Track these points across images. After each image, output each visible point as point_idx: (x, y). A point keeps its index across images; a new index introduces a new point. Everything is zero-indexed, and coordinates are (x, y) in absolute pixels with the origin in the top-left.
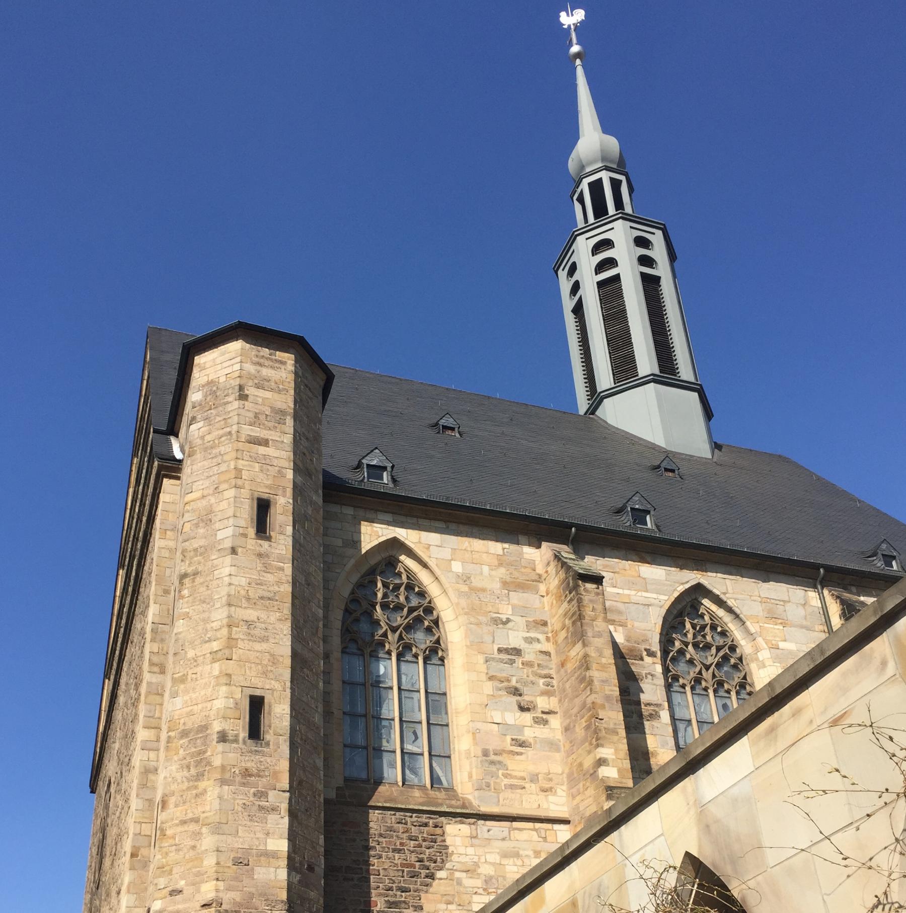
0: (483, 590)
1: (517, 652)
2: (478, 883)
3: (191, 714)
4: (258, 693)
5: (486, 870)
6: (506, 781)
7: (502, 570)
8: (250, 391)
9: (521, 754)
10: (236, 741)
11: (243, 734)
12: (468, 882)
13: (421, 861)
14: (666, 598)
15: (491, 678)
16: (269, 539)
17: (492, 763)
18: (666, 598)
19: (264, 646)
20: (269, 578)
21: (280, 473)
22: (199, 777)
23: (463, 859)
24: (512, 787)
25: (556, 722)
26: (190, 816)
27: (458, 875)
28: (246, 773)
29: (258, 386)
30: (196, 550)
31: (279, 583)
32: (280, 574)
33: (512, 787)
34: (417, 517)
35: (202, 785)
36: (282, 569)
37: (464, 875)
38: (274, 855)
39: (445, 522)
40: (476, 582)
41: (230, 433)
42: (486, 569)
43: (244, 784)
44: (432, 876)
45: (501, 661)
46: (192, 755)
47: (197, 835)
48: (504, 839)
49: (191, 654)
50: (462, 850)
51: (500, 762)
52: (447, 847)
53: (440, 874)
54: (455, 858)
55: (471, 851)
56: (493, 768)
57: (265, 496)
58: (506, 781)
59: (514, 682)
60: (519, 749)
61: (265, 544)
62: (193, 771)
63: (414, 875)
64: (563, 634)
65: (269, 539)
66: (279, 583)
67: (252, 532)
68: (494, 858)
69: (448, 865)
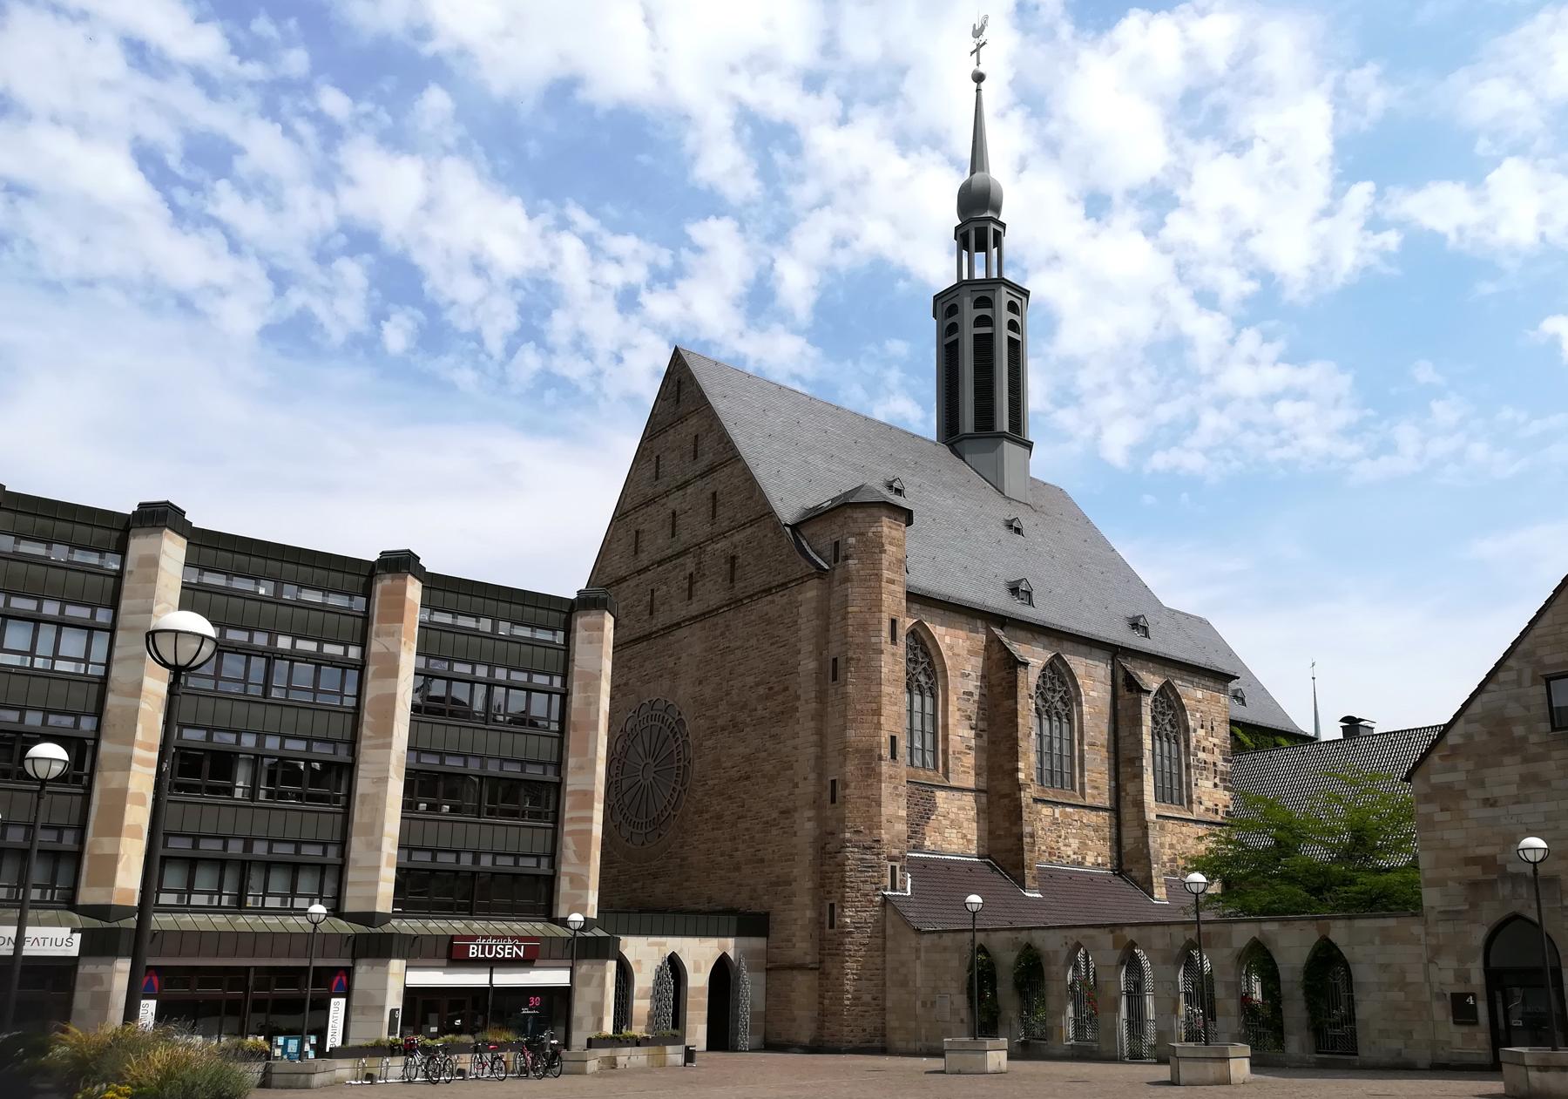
0: (959, 655)
1: (971, 694)
2: (948, 822)
3: (861, 741)
4: (893, 735)
5: (952, 816)
6: (962, 769)
7: (968, 642)
8: (887, 547)
9: (969, 754)
10: (886, 760)
11: (889, 757)
12: (944, 822)
13: (925, 810)
14: (1041, 662)
15: (959, 710)
16: (896, 644)
17: (956, 758)
18: (1041, 662)
19: (895, 708)
20: (897, 668)
21: (900, 602)
22: (868, 776)
23: (943, 810)
24: (964, 772)
25: (985, 736)
26: (864, 794)
27: (940, 818)
28: (891, 777)
29: (890, 544)
30: (857, 644)
31: (900, 671)
32: (901, 666)
33: (964, 772)
34: (931, 607)
35: (870, 781)
36: (901, 663)
37: (942, 818)
38: (901, 818)
39: (944, 610)
40: (956, 651)
41: (877, 574)
42: (961, 641)
43: (890, 783)
44: (929, 818)
45: (964, 699)
46: (864, 764)
47: (869, 806)
48: (959, 800)
49: (858, 707)
50: (942, 805)
51: (959, 758)
52: (936, 803)
53: (933, 817)
54: (939, 809)
55: (945, 806)
56: (957, 761)
57: (894, 617)
58: (962, 769)
59: (968, 713)
60: (969, 751)
61: (895, 647)
62: (865, 772)
63: (922, 817)
64: (999, 689)
65: (896, 644)
66: (900, 671)
67: (889, 639)
68: (955, 810)
69: (936, 813)
